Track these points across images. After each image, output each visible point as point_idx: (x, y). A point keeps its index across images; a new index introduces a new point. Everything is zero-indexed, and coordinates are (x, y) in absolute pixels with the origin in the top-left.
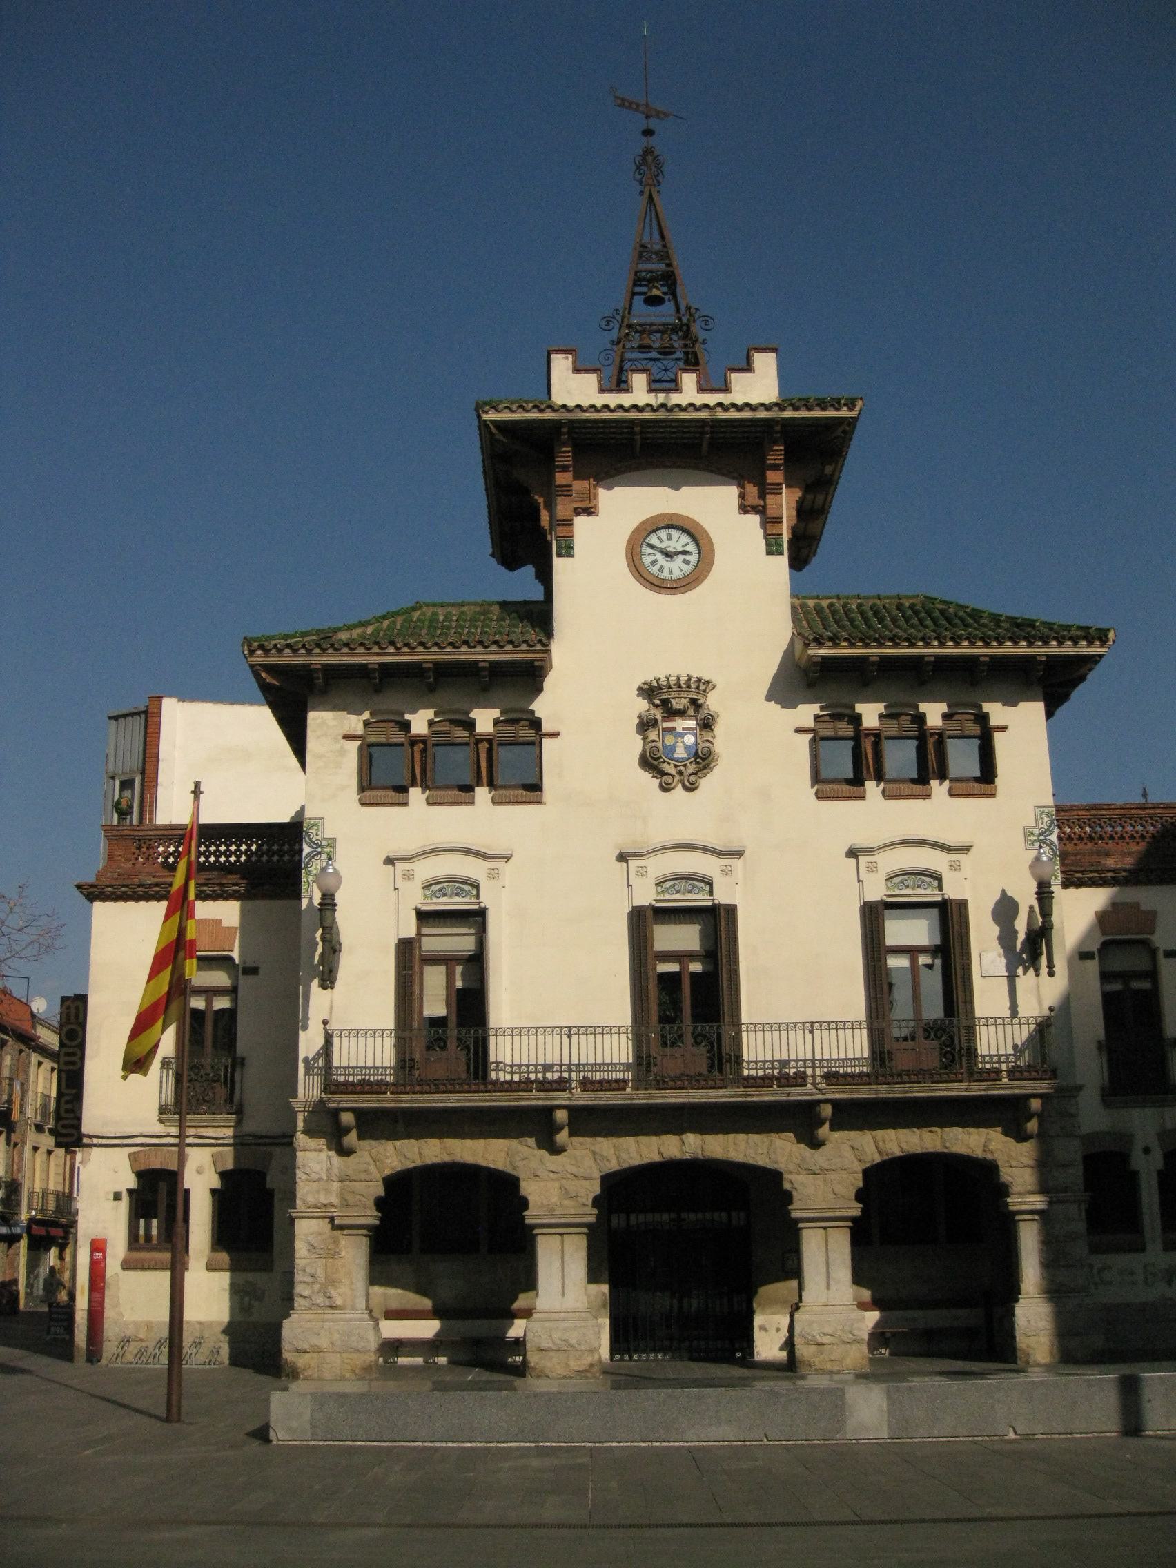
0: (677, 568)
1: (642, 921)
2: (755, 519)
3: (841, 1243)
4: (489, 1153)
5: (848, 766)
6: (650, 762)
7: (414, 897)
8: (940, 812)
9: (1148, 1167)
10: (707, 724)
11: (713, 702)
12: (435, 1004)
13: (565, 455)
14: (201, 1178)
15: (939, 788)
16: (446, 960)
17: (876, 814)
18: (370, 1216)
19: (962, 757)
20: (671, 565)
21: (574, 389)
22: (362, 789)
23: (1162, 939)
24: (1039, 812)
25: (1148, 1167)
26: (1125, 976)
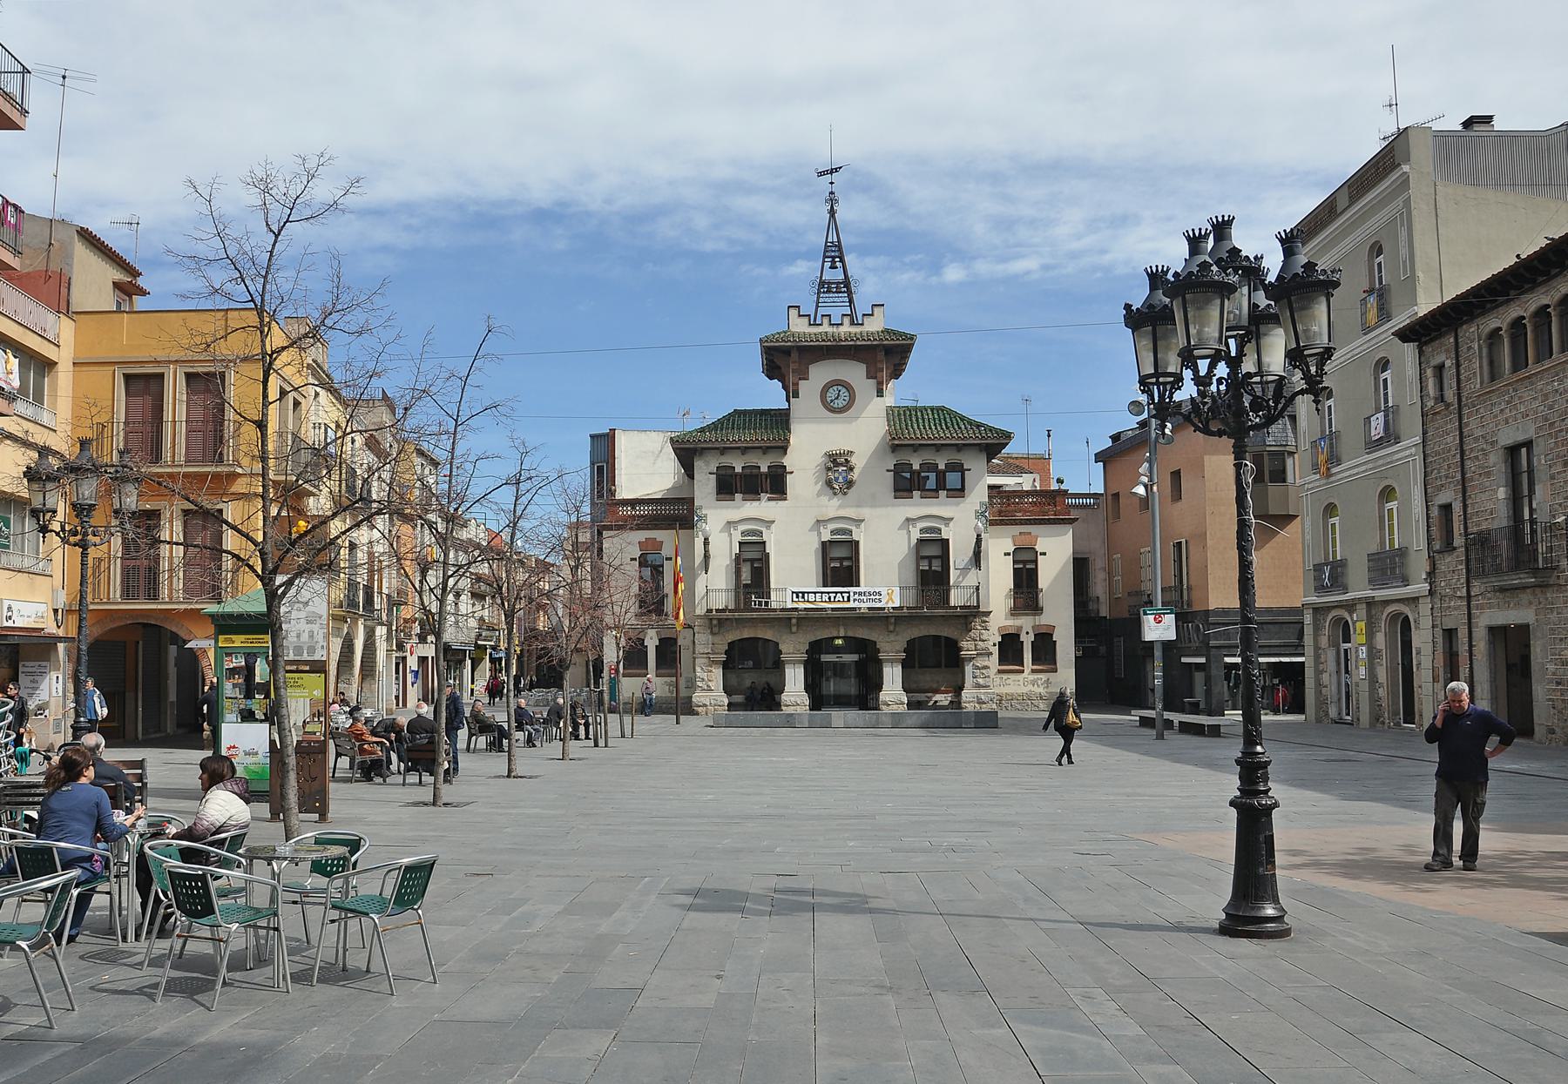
0: (840, 403)
1: (825, 546)
2: (872, 382)
3: (898, 670)
4: (768, 634)
5: (906, 484)
6: (829, 483)
7: (737, 537)
8: (941, 507)
9: (1027, 640)
10: (851, 469)
11: (853, 460)
12: (746, 577)
13: (795, 355)
14: (651, 642)
15: (943, 493)
16: (752, 561)
17: (917, 507)
18: (723, 657)
19: (952, 479)
20: (839, 402)
21: (800, 326)
22: (718, 493)
23: (1039, 548)
24: (982, 504)
25: (1027, 640)
26: (1024, 562)
